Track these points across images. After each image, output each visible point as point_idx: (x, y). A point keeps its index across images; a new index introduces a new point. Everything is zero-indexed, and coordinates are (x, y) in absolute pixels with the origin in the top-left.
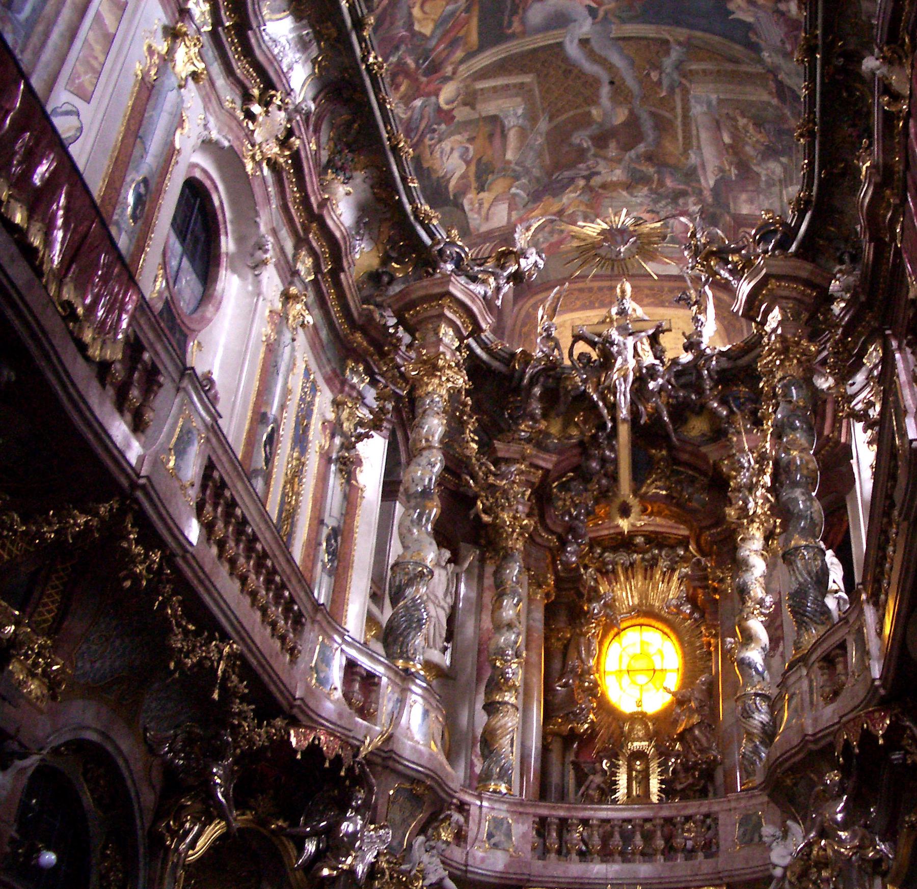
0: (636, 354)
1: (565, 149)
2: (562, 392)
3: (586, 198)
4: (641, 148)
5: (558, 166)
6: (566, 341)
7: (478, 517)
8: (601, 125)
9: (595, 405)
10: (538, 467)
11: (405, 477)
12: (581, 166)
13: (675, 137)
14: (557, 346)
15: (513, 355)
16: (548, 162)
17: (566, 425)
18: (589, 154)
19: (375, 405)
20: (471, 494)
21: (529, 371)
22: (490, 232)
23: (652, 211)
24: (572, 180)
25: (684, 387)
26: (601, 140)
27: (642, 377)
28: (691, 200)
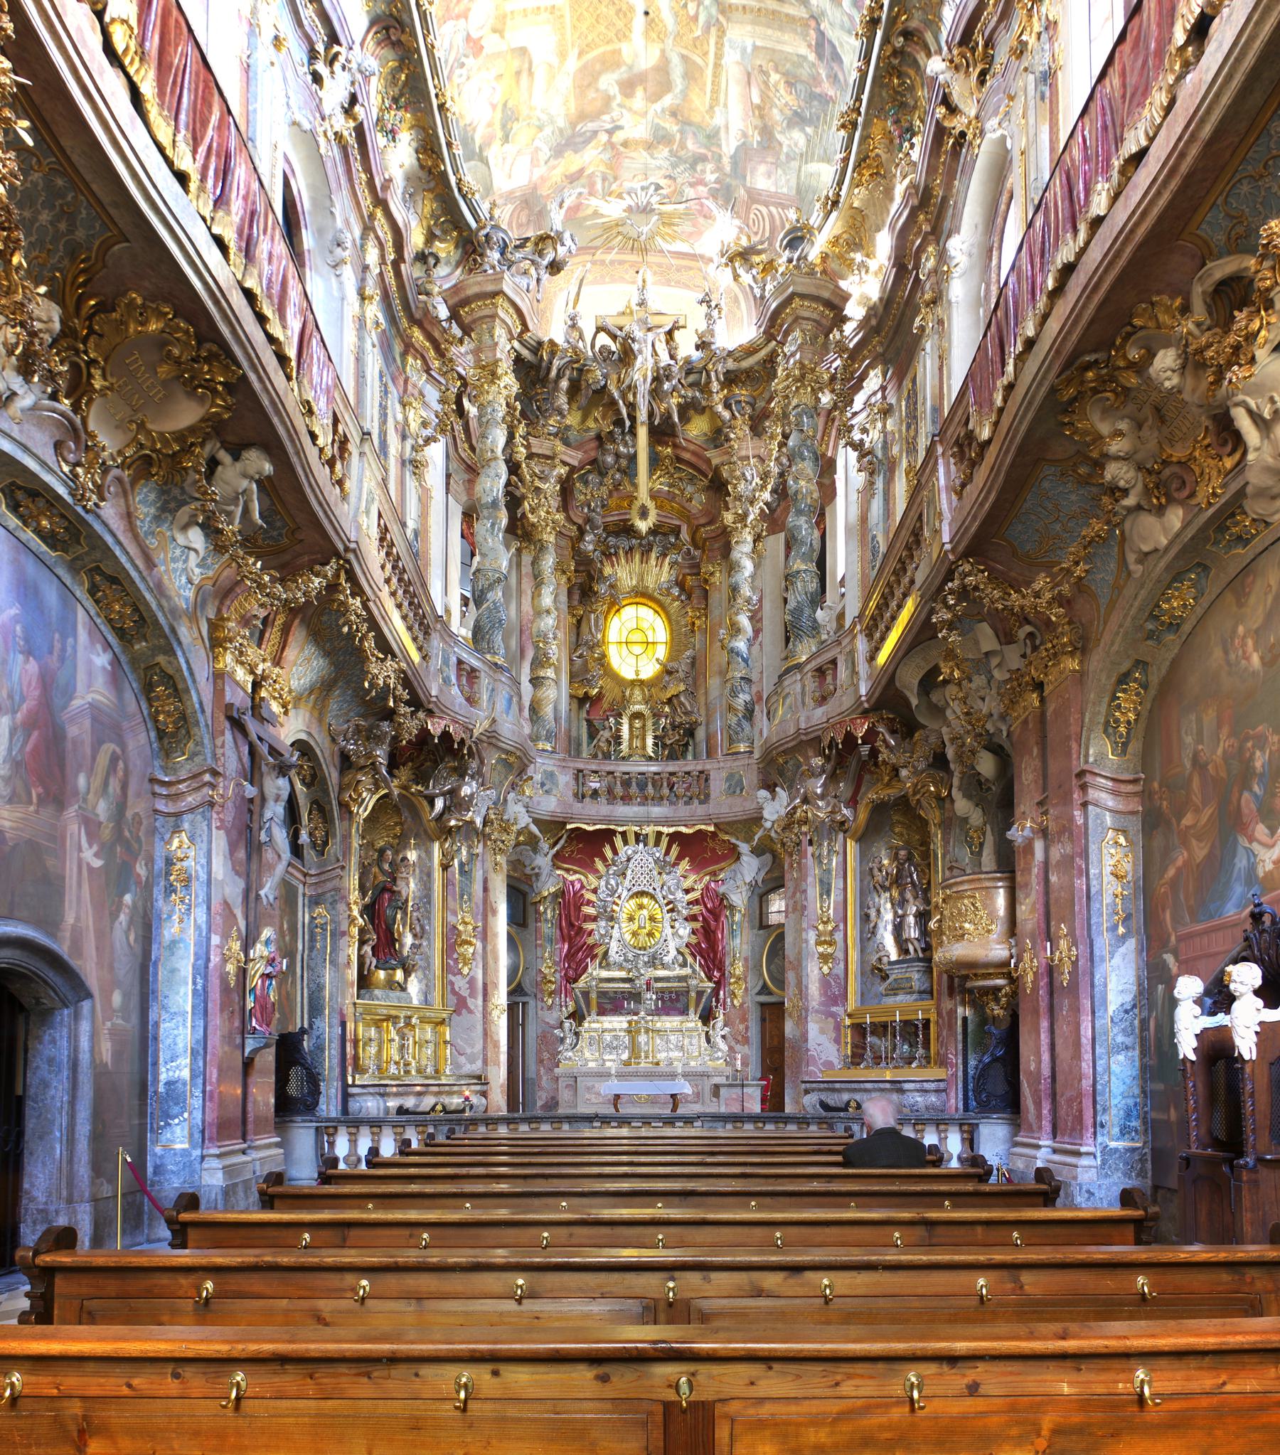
0: (655, 353)
1: (591, 94)
2: (583, 384)
3: (606, 156)
4: (668, 101)
5: (583, 116)
6: (588, 337)
7: (524, 514)
8: (630, 68)
9: (613, 403)
10: (565, 463)
11: (478, 488)
12: (606, 117)
13: (703, 90)
14: (581, 337)
15: (540, 344)
16: (573, 111)
17: (584, 419)
18: (614, 104)
19: (438, 407)
20: (518, 494)
21: (556, 363)
22: (511, 192)
23: (670, 177)
24: (595, 133)
25: (691, 385)
26: (628, 87)
27: (656, 379)
28: (710, 167)
